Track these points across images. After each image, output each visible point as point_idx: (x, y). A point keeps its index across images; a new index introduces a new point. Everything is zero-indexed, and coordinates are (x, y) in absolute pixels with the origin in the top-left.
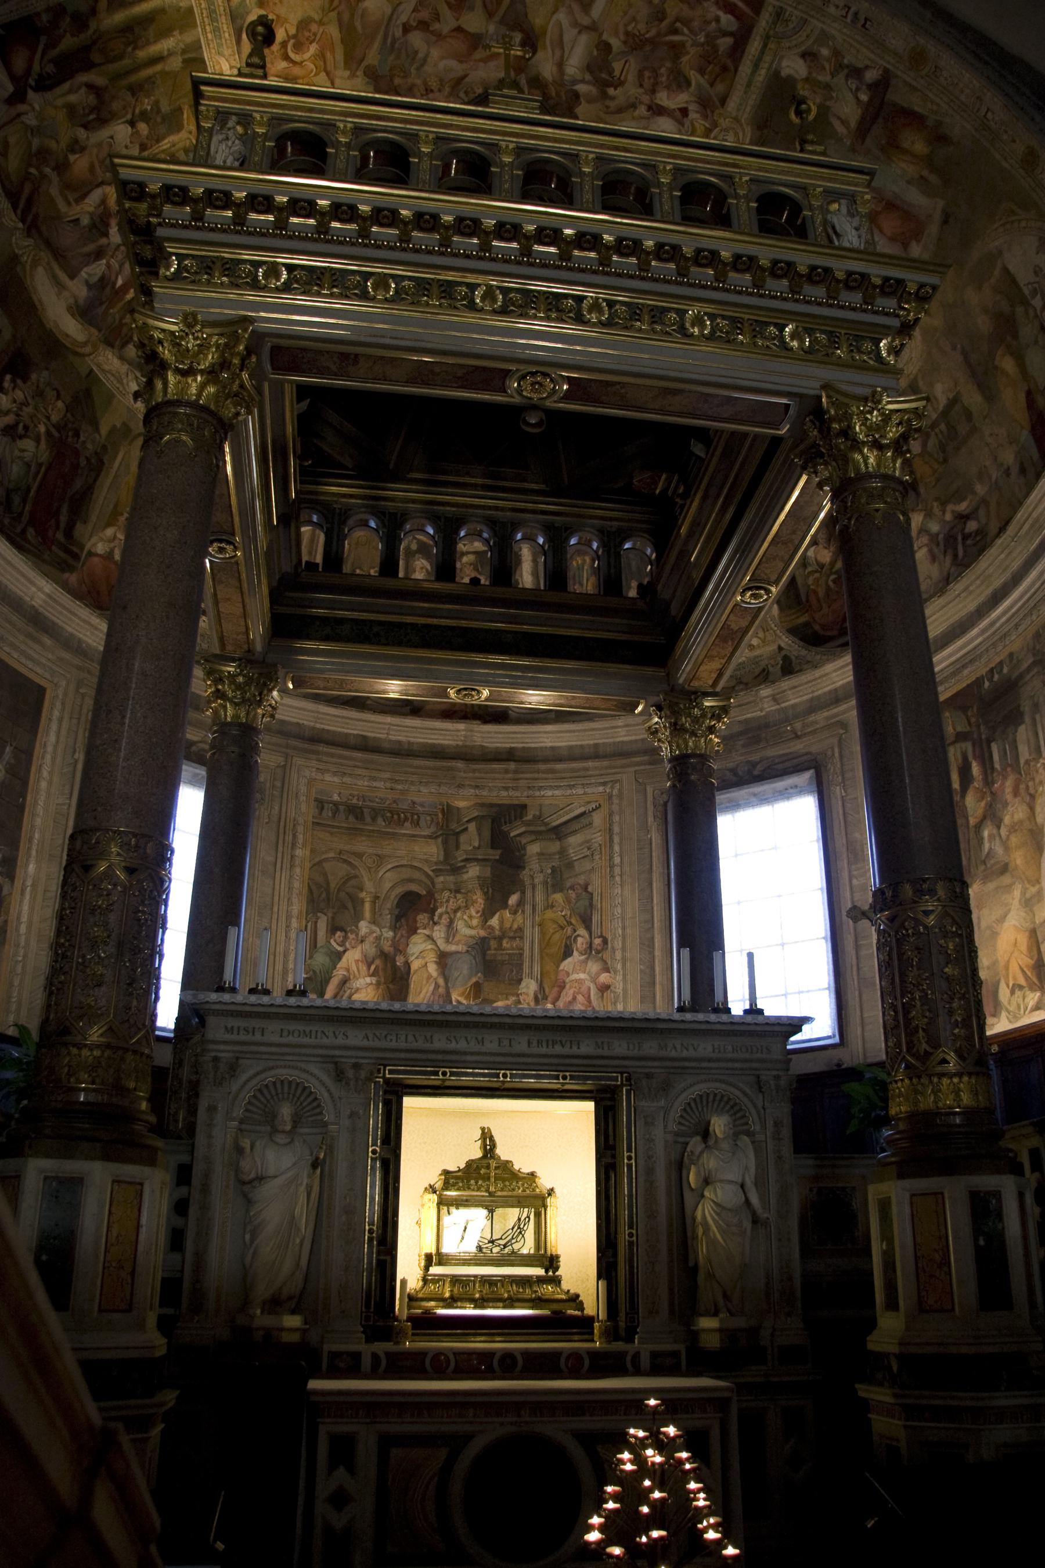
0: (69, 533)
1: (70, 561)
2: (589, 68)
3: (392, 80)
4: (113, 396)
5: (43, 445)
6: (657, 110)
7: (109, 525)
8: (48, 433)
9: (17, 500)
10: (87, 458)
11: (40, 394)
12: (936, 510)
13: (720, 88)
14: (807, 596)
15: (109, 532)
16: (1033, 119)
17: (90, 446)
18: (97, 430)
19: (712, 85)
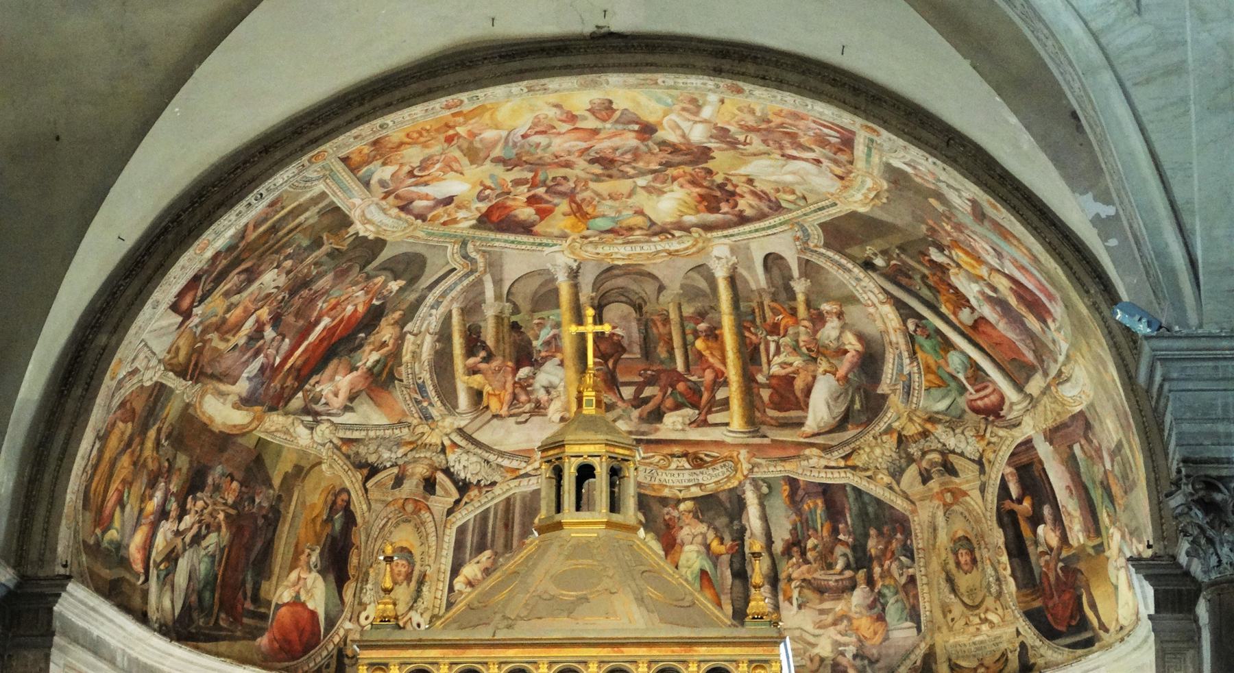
0: (256, 599)
1: (260, 624)
2: (711, 137)
3: (520, 159)
4: (279, 450)
5: (224, 529)
6: (795, 158)
7: (292, 568)
8: (227, 516)
9: (207, 595)
10: (265, 517)
11: (217, 488)
12: (1128, 537)
13: (842, 157)
14: (1041, 579)
15: (293, 576)
16: (1087, 292)
17: (266, 504)
18: (271, 486)
19: (835, 154)
